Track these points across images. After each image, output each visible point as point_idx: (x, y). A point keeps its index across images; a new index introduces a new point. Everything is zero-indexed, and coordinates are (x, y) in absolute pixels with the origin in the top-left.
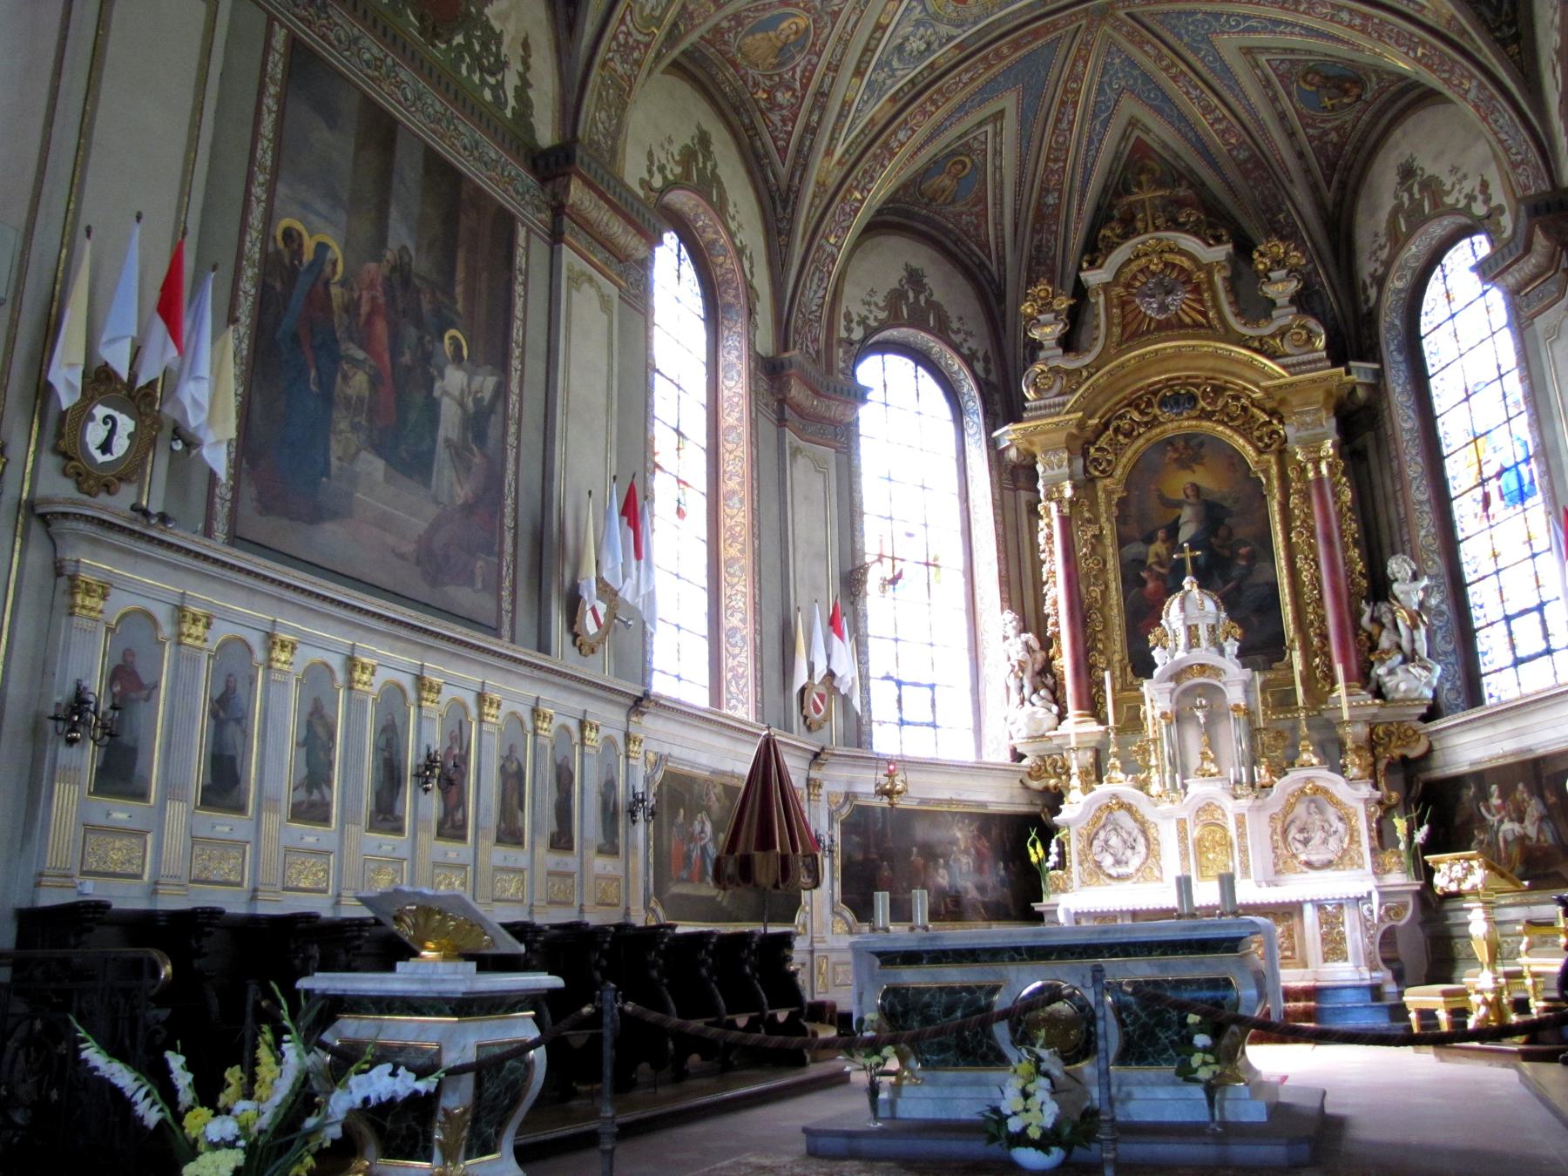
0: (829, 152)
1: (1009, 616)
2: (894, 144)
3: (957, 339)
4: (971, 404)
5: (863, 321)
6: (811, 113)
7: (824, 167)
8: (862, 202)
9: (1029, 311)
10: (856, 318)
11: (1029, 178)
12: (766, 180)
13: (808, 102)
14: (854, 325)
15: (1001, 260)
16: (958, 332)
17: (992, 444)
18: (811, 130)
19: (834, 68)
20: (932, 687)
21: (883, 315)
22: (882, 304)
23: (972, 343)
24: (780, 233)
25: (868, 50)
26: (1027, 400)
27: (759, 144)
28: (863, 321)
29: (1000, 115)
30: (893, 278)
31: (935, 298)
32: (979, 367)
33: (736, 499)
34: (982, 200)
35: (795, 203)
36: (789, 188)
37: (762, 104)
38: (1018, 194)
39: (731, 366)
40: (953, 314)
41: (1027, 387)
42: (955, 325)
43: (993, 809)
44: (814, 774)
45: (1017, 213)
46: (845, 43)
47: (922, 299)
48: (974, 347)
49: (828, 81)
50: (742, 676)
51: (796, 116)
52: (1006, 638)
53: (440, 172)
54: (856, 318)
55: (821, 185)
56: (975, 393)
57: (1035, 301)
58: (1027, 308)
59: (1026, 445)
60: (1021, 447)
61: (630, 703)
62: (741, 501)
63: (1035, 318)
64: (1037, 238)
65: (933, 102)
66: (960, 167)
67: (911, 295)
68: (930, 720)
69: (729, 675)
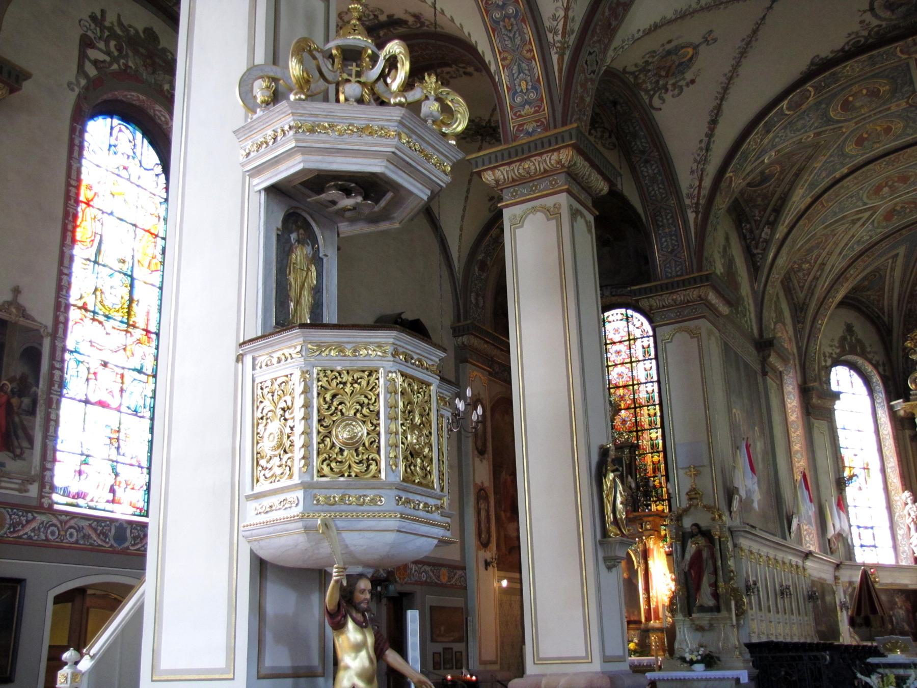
0: (822, 287)
1: (907, 494)
2: (848, 276)
3: (870, 356)
4: (877, 387)
5: (831, 355)
6: (818, 271)
7: (819, 292)
8: (832, 303)
9: (909, 345)
10: (827, 355)
11: (907, 279)
12: (793, 299)
13: (815, 268)
14: (827, 358)
15: (890, 316)
16: (870, 353)
17: (891, 409)
18: (816, 278)
19: (830, 254)
20: (872, 528)
21: (838, 351)
22: (837, 345)
23: (877, 358)
24: (799, 323)
25: (846, 244)
26: (911, 390)
27: (791, 285)
28: (831, 355)
29: (897, 255)
30: (840, 331)
31: (859, 337)
32: (881, 369)
33: (799, 455)
34: (883, 289)
35: (806, 310)
36: (804, 303)
37: (795, 269)
38: (901, 286)
39: (790, 393)
40: (867, 345)
41: (911, 383)
42: (869, 349)
43: (911, 587)
44: (837, 574)
45: (900, 295)
46: (836, 244)
47: (853, 339)
48: (878, 359)
49: (826, 259)
50: (811, 533)
51: (809, 274)
52: (906, 504)
53: (746, 365)
54: (827, 355)
55: (818, 299)
56: (880, 382)
57: (912, 340)
58: (908, 344)
59: (910, 410)
60: (908, 411)
61: (803, 555)
62: (802, 455)
63: (913, 349)
64: (909, 305)
65: (868, 256)
66: (873, 277)
67: (848, 337)
68: (873, 544)
69: (805, 533)
